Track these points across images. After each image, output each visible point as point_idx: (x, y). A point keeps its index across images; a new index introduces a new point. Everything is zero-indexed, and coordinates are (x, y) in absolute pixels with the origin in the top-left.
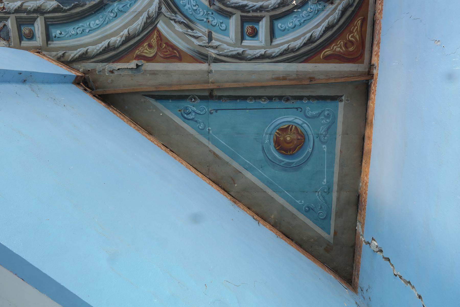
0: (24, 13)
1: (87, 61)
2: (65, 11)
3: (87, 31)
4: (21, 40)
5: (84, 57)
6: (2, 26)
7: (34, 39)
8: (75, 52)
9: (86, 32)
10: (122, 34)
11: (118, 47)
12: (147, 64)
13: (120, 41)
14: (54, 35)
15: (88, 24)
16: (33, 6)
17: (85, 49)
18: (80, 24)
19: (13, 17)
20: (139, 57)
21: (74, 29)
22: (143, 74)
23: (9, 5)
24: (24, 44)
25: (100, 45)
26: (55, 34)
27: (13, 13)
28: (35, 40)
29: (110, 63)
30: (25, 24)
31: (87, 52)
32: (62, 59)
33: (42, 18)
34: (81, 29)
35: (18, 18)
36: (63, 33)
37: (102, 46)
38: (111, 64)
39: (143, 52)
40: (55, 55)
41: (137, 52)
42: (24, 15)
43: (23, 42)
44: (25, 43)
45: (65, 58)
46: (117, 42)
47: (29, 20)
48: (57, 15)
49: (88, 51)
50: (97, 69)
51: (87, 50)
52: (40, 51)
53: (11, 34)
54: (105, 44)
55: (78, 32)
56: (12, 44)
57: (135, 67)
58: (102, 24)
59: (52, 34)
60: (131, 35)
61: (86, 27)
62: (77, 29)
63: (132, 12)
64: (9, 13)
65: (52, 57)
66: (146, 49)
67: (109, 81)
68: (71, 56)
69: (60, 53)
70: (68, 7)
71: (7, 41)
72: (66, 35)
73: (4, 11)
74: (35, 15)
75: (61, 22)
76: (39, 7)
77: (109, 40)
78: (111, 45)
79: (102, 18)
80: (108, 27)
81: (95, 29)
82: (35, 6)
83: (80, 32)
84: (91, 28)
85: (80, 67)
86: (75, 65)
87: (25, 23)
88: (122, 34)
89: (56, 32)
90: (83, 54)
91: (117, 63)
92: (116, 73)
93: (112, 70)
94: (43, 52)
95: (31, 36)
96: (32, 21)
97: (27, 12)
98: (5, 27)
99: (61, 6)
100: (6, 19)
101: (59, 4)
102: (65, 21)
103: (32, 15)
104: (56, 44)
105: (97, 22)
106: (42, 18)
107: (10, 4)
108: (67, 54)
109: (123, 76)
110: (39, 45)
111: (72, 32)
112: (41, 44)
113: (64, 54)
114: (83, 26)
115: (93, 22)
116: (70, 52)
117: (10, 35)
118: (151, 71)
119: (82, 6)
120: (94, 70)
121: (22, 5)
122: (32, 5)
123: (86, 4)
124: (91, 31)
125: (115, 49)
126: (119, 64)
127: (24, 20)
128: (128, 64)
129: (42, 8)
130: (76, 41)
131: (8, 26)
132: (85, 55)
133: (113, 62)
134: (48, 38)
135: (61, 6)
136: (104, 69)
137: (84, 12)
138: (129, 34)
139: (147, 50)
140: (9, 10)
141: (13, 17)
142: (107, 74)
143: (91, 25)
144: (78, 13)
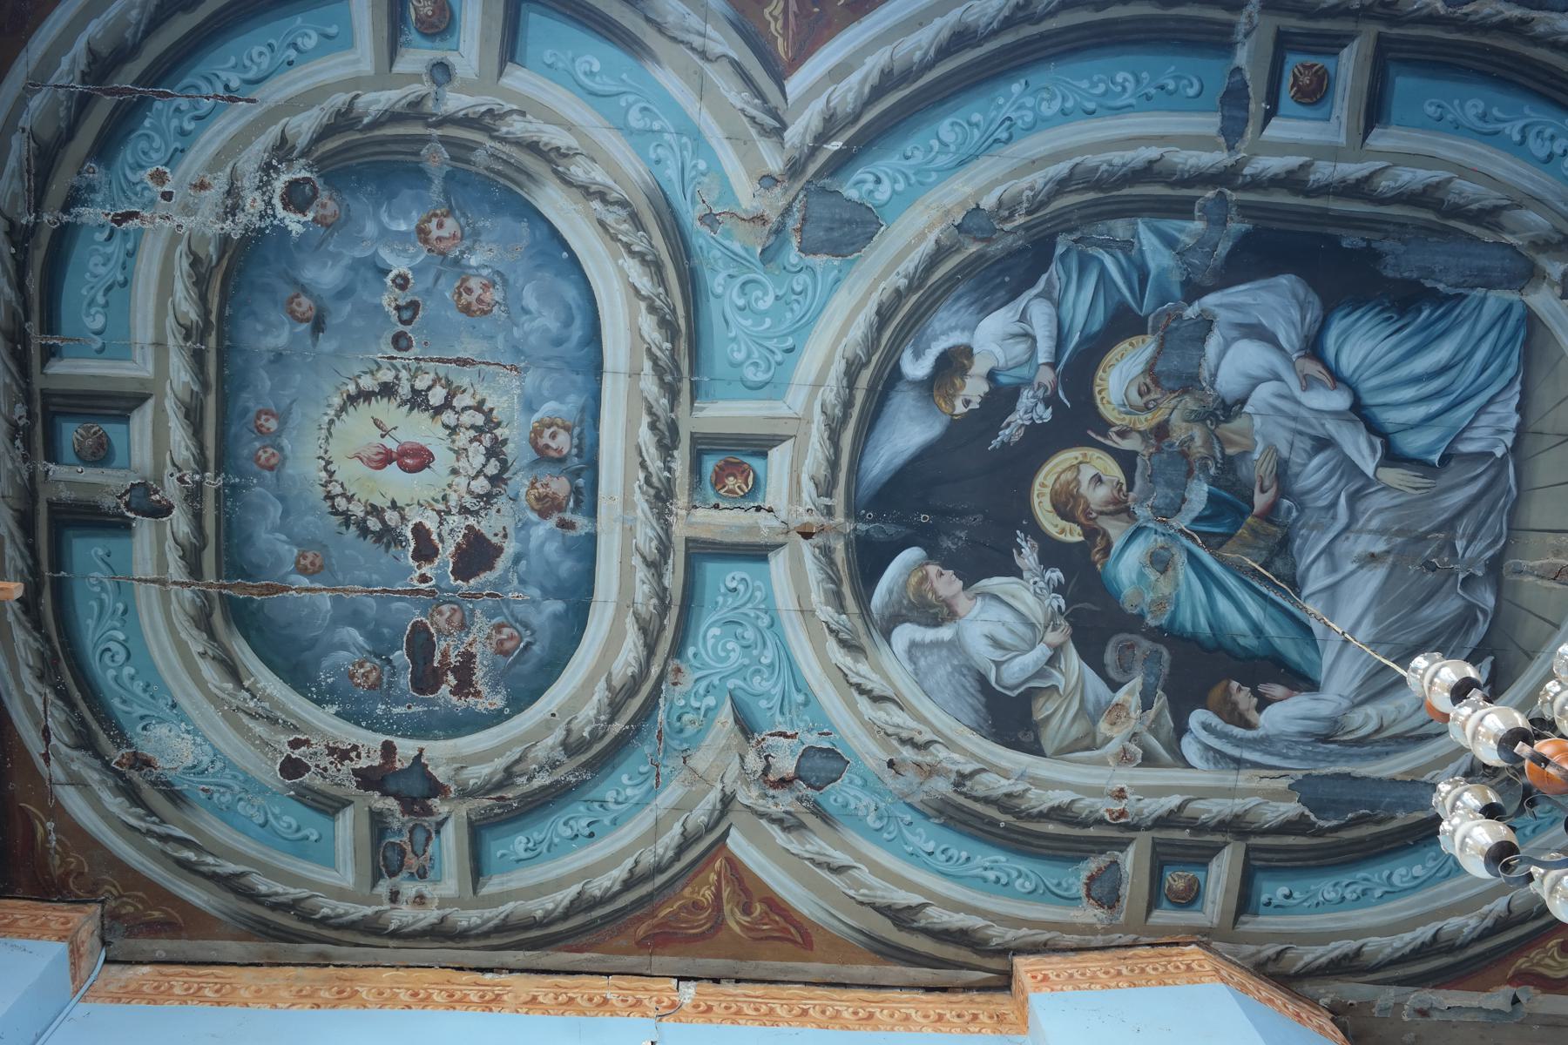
0: (1184, 828)
1: (1351, 979)
2: (1321, 832)
3: (1378, 893)
4: (1153, 904)
5: (1346, 967)
6: (1102, 865)
7: (1198, 906)
8: (1320, 950)
9: (1373, 897)
10: (1486, 908)
11: (1465, 946)
12: (1541, 997)
13: (1475, 928)
14: (1264, 898)
15: (1386, 873)
16: (1219, 812)
17: (1355, 945)
18: (1360, 875)
19: (1143, 840)
20: (1523, 978)
21: (1335, 885)
22: (1521, 1023)
23: (1141, 804)
24: (1158, 917)
25: (1408, 937)
26: (1268, 896)
27: (1148, 829)
28: (1201, 911)
29: (1424, 987)
30: (1180, 863)
31: (1358, 952)
32: (1271, 968)
33: (1240, 847)
34: (1359, 888)
35: (1159, 844)
36: (1296, 895)
37: (1414, 939)
38: (1427, 991)
39: (1538, 964)
40: (1253, 955)
41: (1522, 963)
42: (1185, 835)
43: (1156, 913)
44: (1164, 916)
45: (1281, 965)
46: (1466, 930)
47: (1195, 852)
48: (1290, 840)
49: (1364, 949)
50: (1379, 1002)
51: (1361, 947)
52: (1205, 939)
53: (1125, 890)
54: (1424, 933)
55: (1348, 896)
56: (1122, 917)
57: (1507, 1008)
58: (1429, 878)
59: (1259, 896)
60: (1516, 910)
61: (1378, 884)
62: (1347, 885)
63: (1536, 848)
64: (1135, 827)
65: (1241, 959)
66: (1552, 957)
67: (1409, 1037)
68: (1301, 958)
69: (1270, 950)
70: (1334, 823)
71: (1110, 908)
72: (1305, 900)
73: (1122, 820)
74: (1218, 838)
75: (1299, 863)
76: (1237, 816)
77: (1439, 925)
78: (1443, 936)
79: (1435, 860)
80: (1447, 886)
81: (1405, 890)
82: (1227, 811)
83: (1355, 896)
84: (1392, 885)
85: (1322, 991)
86: (1308, 988)
87: (1178, 859)
88: (1486, 908)
89: (1273, 890)
90: (1345, 956)
91: (1448, 988)
92: (1436, 1017)
93: (1426, 1007)
94: (1215, 944)
95: (1190, 898)
96: (1202, 856)
97: (1191, 828)
98: (1114, 868)
99: (1313, 817)
100: (1122, 845)
101: (1307, 812)
102: (1313, 863)
103: (1208, 838)
104: (1262, 923)
105: (1417, 870)
106: (1240, 847)
107: (1147, 801)
108: (1289, 954)
109: (1454, 1027)
110: (1209, 925)
111: (1326, 896)
112: (1216, 921)
113: (1280, 954)
114: (1366, 879)
115: (1403, 871)
116: (1302, 949)
117: (1121, 891)
118: (1546, 1016)
119: (1379, 822)
120: (1370, 1004)
121: (1181, 807)
122: (1215, 810)
123: (1393, 818)
124: (1392, 893)
125: (1452, 948)
126: (1453, 992)
127: (1177, 850)
128: (1485, 994)
129: (1249, 818)
130: (1331, 920)
131: (1121, 866)
132: (1351, 960)
133: (1435, 987)
134: (1245, 903)
135: (1313, 817)
136: (1399, 1006)
137: (1378, 838)
138: (1509, 910)
139: (1555, 960)
140: (1136, 819)
141: (1143, 840)
142: (1405, 1018)
143: (1396, 879)
144: (1360, 841)
